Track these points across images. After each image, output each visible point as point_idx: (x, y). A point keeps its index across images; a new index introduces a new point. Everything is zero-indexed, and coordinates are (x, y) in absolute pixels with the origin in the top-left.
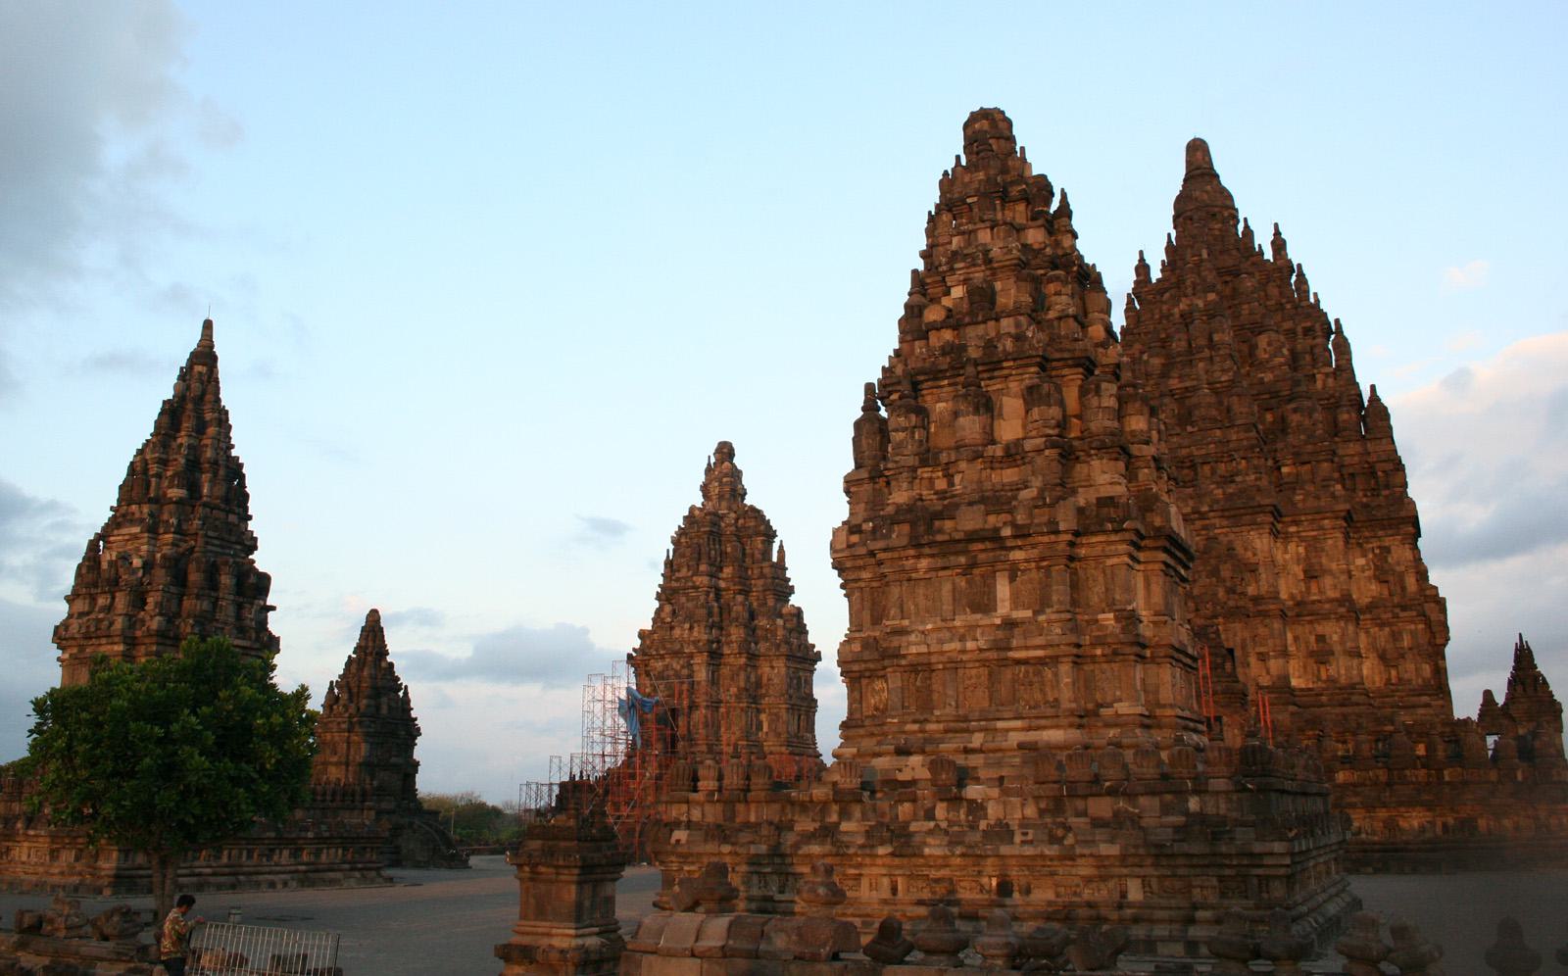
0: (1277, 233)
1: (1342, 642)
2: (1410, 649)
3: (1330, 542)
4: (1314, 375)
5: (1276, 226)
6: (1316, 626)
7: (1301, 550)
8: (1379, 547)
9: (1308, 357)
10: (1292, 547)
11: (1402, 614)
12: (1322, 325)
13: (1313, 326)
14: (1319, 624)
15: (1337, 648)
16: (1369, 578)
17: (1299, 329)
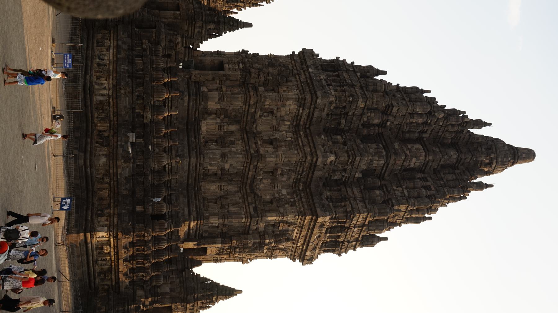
0: (487, 186)
1: (230, 152)
2: (228, 211)
4: (401, 186)
5: (492, 186)
6: (241, 141)
7: (289, 139)
8: (295, 201)
9: (412, 185)
10: (290, 134)
11: (251, 207)
12: (434, 195)
13: (431, 190)
14: (242, 143)
15: (226, 150)
16: (273, 195)
17: (428, 184)
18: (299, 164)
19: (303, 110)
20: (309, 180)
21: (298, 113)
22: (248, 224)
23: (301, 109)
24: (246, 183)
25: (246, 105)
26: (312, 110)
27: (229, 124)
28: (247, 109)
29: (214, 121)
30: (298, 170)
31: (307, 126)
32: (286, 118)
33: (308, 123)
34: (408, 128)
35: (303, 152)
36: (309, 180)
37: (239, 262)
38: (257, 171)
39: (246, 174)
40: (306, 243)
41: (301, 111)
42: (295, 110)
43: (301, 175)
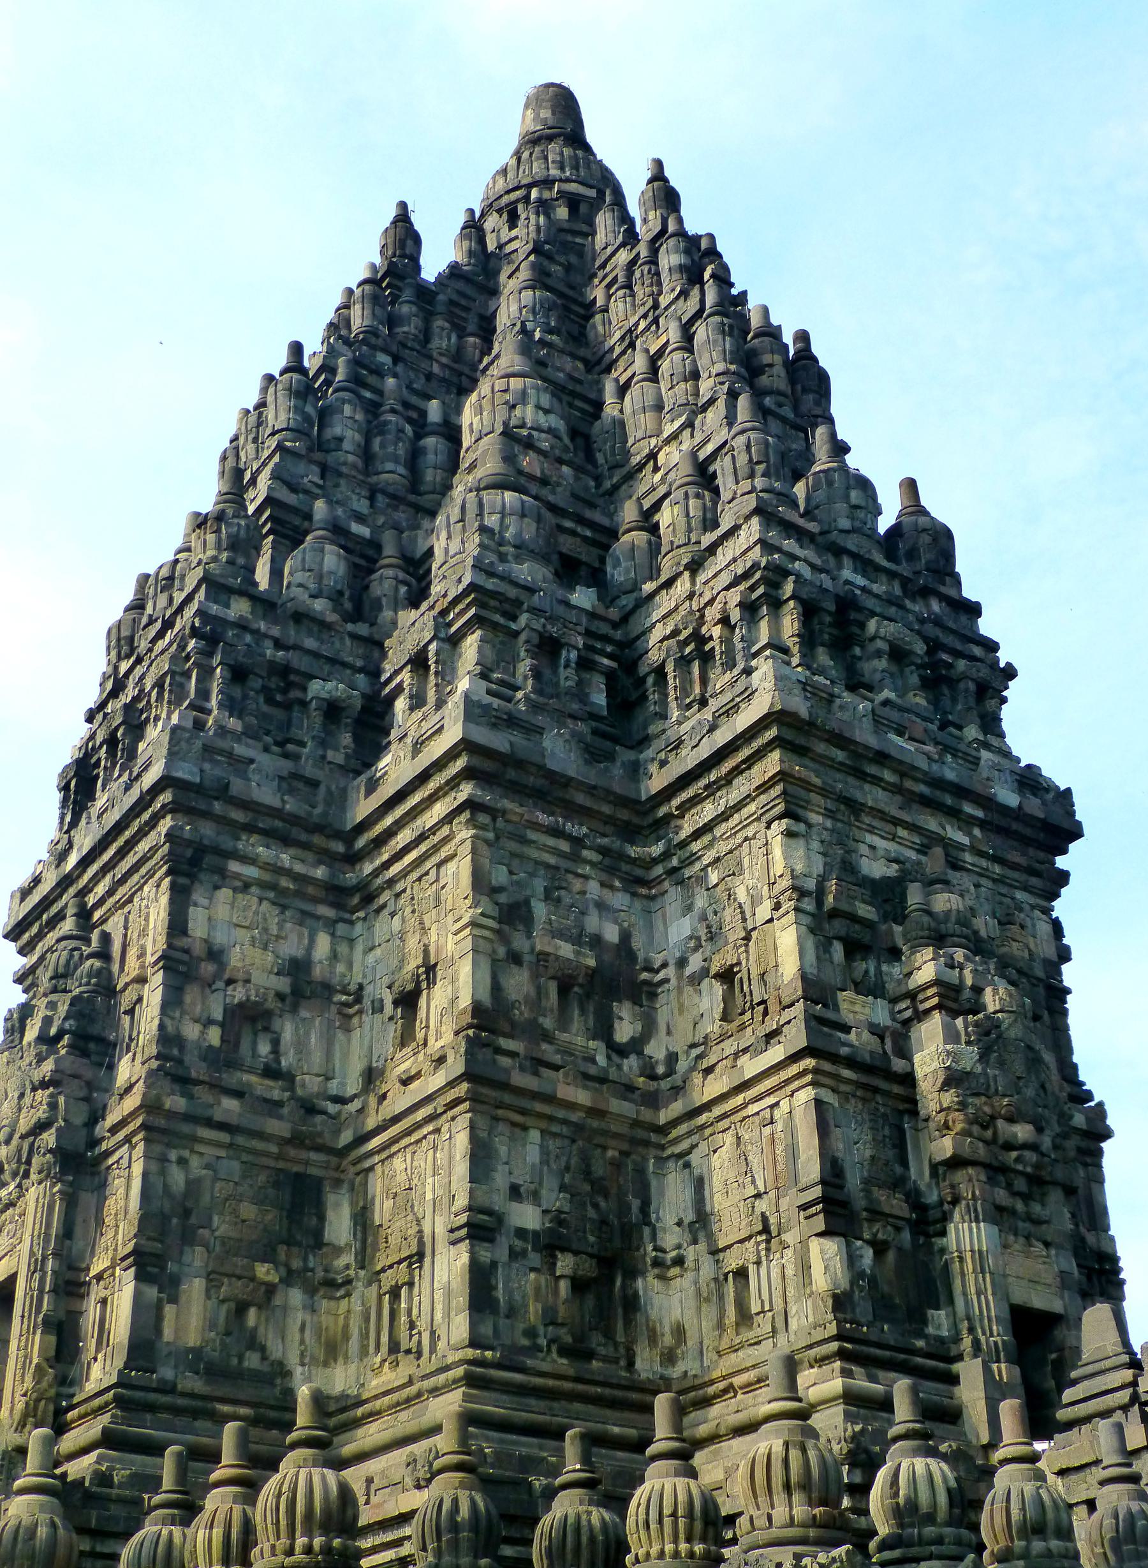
3: (451, 866)
18: (512, 846)
19: (245, 859)
20: (606, 809)
21: (263, 885)
22: (847, 1073)
23: (234, 866)
24: (636, 1123)
25: (195, 1139)
26: (238, 815)
27: (317, 1241)
28: (224, 1137)
29: (298, 1317)
30: (552, 860)
31: (339, 847)
32: (291, 947)
33: (317, 840)
34: (389, 466)
35: (445, 831)
36: (606, 809)
37: (1107, 1162)
38: (557, 1059)
39: (575, 1117)
40: (949, 800)
41: (251, 872)
42: (250, 900)
43: (577, 842)
